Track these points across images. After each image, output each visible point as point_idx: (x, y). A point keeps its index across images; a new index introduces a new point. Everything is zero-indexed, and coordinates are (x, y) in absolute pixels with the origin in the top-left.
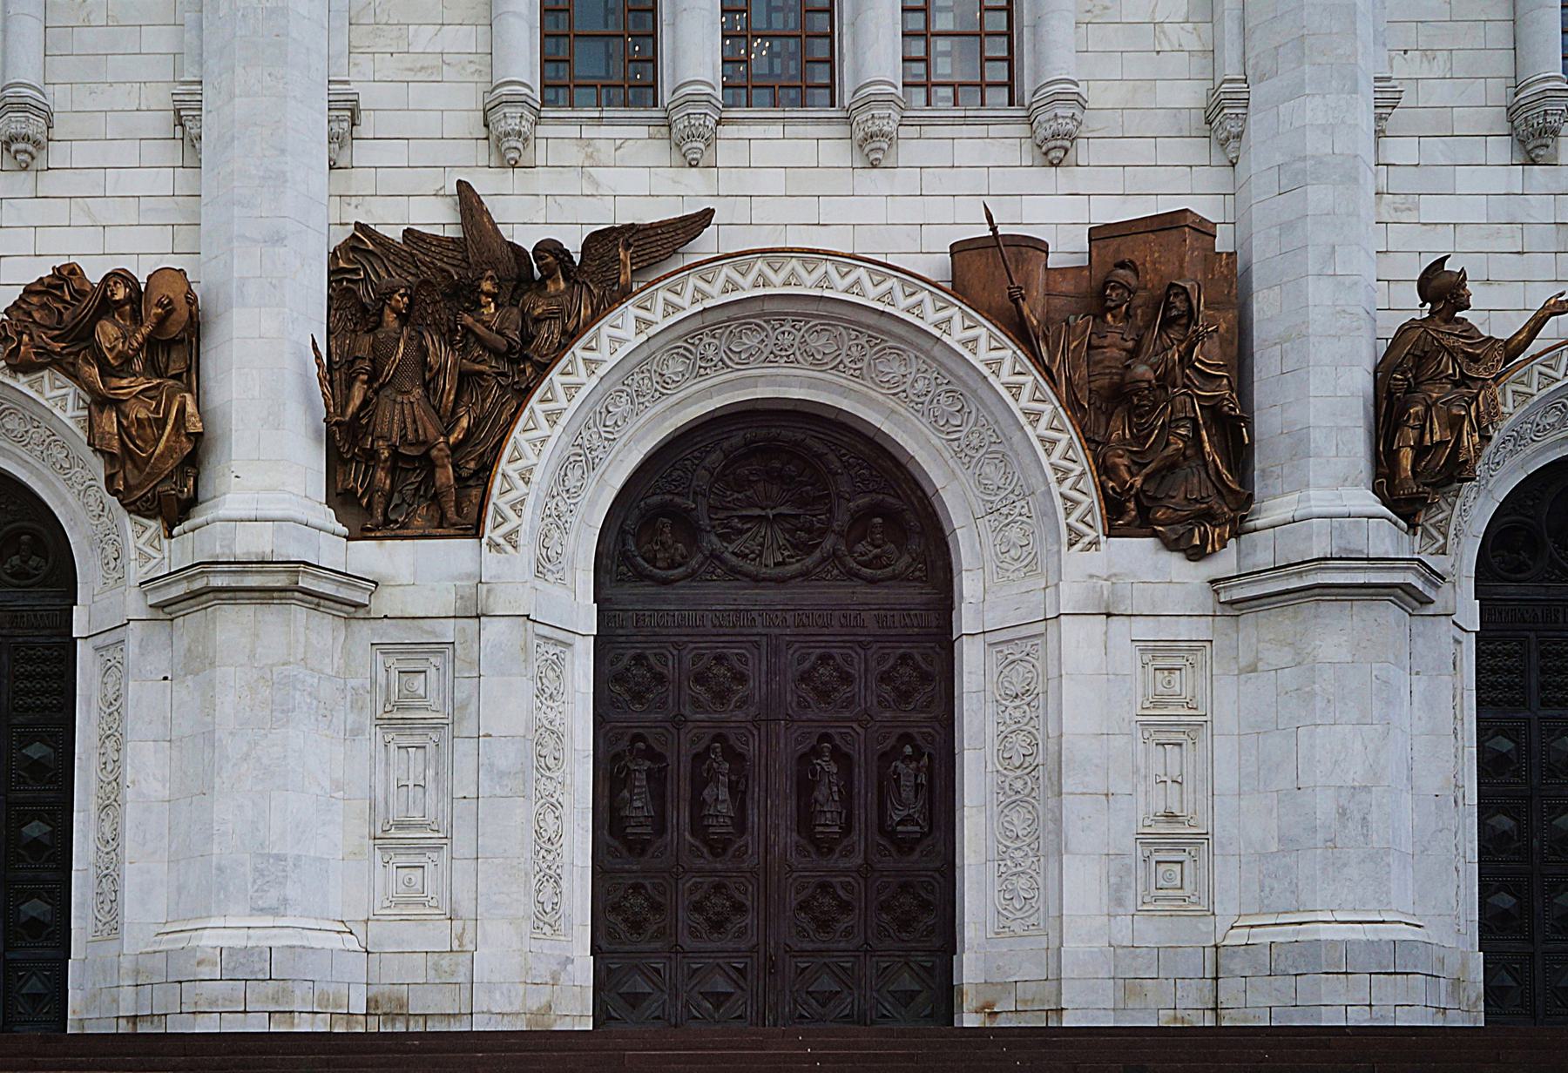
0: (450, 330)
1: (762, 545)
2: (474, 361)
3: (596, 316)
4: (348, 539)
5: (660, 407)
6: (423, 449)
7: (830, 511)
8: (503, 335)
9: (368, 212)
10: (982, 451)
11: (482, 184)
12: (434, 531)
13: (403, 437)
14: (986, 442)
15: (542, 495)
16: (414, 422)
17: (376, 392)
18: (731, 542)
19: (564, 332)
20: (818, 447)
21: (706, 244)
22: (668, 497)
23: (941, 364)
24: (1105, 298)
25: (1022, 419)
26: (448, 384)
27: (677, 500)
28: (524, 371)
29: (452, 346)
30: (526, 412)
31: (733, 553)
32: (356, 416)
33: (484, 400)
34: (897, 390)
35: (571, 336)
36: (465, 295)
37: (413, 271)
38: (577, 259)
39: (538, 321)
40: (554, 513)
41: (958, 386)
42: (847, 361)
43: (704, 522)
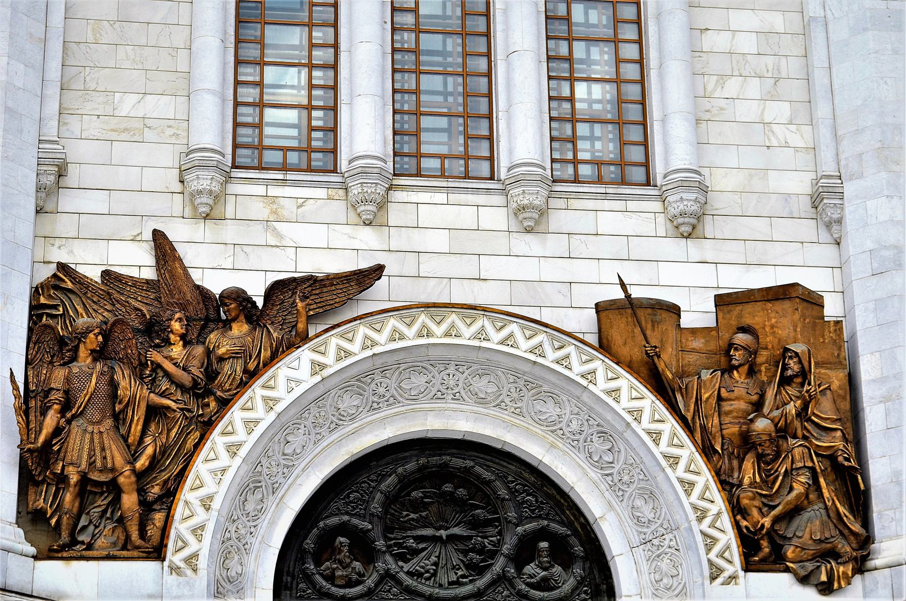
0: (141, 364)
1: (436, 564)
2: (162, 395)
3: (275, 357)
4: (36, 558)
5: (335, 436)
6: (110, 476)
7: (500, 533)
8: (189, 372)
9: (71, 252)
10: (633, 487)
11: (176, 232)
12: (118, 553)
13: (91, 464)
14: (636, 478)
15: (222, 520)
16: (103, 449)
17: (69, 422)
18: (407, 561)
19: (245, 371)
20: (487, 475)
21: (380, 294)
22: (346, 518)
23: (591, 409)
24: (730, 358)
25: (663, 463)
26: (139, 416)
27: (355, 521)
28: (208, 405)
29: (142, 378)
30: (208, 444)
31: (409, 574)
32: (48, 443)
33: (169, 431)
34: (553, 426)
35: (252, 375)
36: (154, 331)
37: (108, 307)
38: (260, 303)
39: (221, 359)
40: (234, 535)
41: (601, 435)
42: (507, 400)
43: (380, 544)
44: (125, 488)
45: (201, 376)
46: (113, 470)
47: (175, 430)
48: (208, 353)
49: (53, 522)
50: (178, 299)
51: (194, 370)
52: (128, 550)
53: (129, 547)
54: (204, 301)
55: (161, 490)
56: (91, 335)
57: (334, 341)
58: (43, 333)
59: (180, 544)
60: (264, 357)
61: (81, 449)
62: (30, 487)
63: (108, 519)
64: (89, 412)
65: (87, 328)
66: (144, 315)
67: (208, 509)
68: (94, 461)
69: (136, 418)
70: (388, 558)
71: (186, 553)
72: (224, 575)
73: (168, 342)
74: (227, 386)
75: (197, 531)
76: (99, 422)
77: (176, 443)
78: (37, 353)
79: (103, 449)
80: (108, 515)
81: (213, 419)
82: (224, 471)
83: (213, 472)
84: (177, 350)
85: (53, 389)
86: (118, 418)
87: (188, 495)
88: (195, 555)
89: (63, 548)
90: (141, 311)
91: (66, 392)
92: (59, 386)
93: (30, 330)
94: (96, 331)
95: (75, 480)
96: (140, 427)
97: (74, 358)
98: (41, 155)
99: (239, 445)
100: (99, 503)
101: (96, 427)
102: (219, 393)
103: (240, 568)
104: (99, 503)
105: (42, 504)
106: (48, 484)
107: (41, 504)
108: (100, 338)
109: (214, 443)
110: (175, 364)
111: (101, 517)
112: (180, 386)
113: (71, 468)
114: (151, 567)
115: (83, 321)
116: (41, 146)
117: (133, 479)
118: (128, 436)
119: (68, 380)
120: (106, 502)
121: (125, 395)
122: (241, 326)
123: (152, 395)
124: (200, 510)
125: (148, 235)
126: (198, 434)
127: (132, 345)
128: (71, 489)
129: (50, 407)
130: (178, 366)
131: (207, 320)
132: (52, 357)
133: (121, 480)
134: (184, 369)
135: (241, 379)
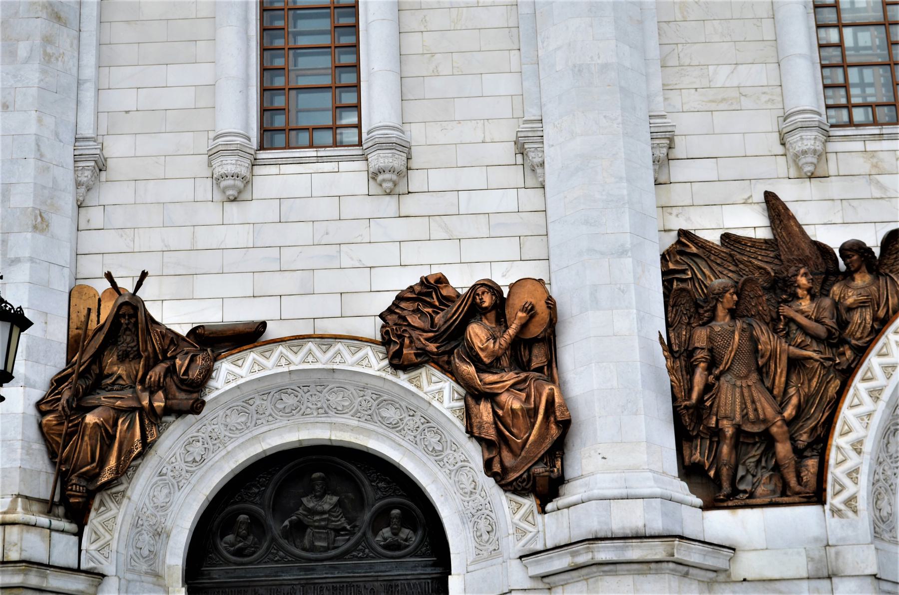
44: (778, 437)
45: (835, 326)
46: (765, 421)
47: (815, 380)
48: (836, 305)
49: (712, 473)
50: (798, 256)
51: (827, 321)
52: (787, 496)
53: (789, 493)
54: (822, 256)
55: (809, 437)
56: (728, 295)
58: (678, 296)
59: (838, 488)
60: (893, 304)
61: (734, 403)
62: (684, 442)
63: (764, 468)
64: (736, 367)
65: (723, 289)
66: (769, 273)
67: (859, 452)
68: (747, 414)
69: (779, 371)
71: (845, 495)
72: (878, 515)
73: (795, 297)
74: (858, 335)
75: (853, 474)
76: (746, 377)
77: (818, 392)
78: (675, 316)
79: (753, 402)
80: (763, 464)
81: (853, 366)
82: (869, 415)
83: (860, 417)
85: (697, 348)
86: (762, 372)
87: (839, 441)
88: (853, 498)
89: (728, 497)
90: (765, 269)
91: (711, 350)
92: (704, 345)
93: (666, 296)
94: (732, 291)
95: (730, 432)
96: (783, 379)
97: (713, 318)
98: (653, 130)
99: (881, 390)
100: (753, 453)
101: (744, 381)
102: (853, 342)
103: (889, 508)
104: (753, 453)
105: (699, 458)
106: (702, 438)
107: (697, 457)
108: (735, 297)
109: (856, 389)
110: (806, 317)
111: (757, 466)
112: (816, 338)
113: (725, 422)
114: (810, 512)
115: (717, 283)
116: (652, 121)
117: (785, 428)
118: (773, 388)
119: (710, 339)
120: (759, 452)
121: (766, 350)
122: (864, 276)
123: (791, 348)
124: (853, 454)
125: (761, 198)
126: (838, 382)
127: (763, 303)
128: (728, 441)
129: (697, 366)
130: (810, 319)
131: (828, 273)
132: (690, 318)
133: (774, 430)
134: (817, 321)
135: (872, 327)
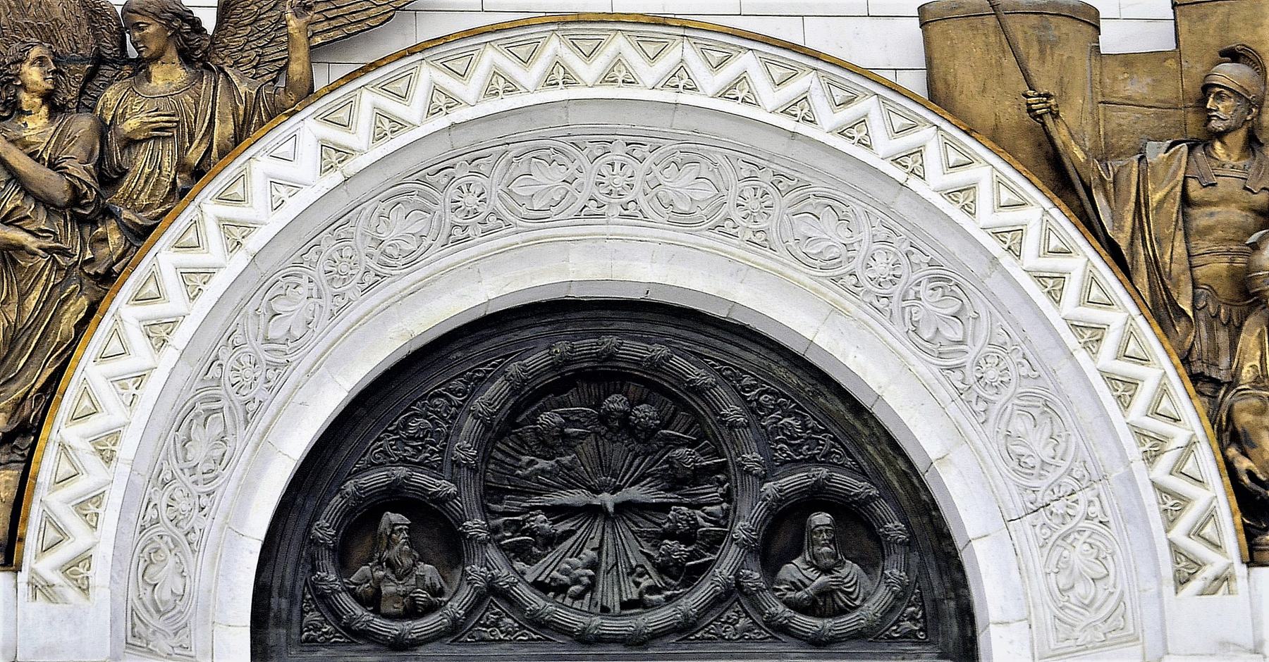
1: (594, 565)
3: (241, 136)
5: (375, 299)
18: (531, 559)
19: (181, 166)
22: (401, 471)
27: (421, 478)
30: (107, 323)
31: (538, 586)
38: (209, 21)
39: (130, 143)
43: (475, 525)
57: (368, 99)
70: (493, 554)
84: (36, 126)
